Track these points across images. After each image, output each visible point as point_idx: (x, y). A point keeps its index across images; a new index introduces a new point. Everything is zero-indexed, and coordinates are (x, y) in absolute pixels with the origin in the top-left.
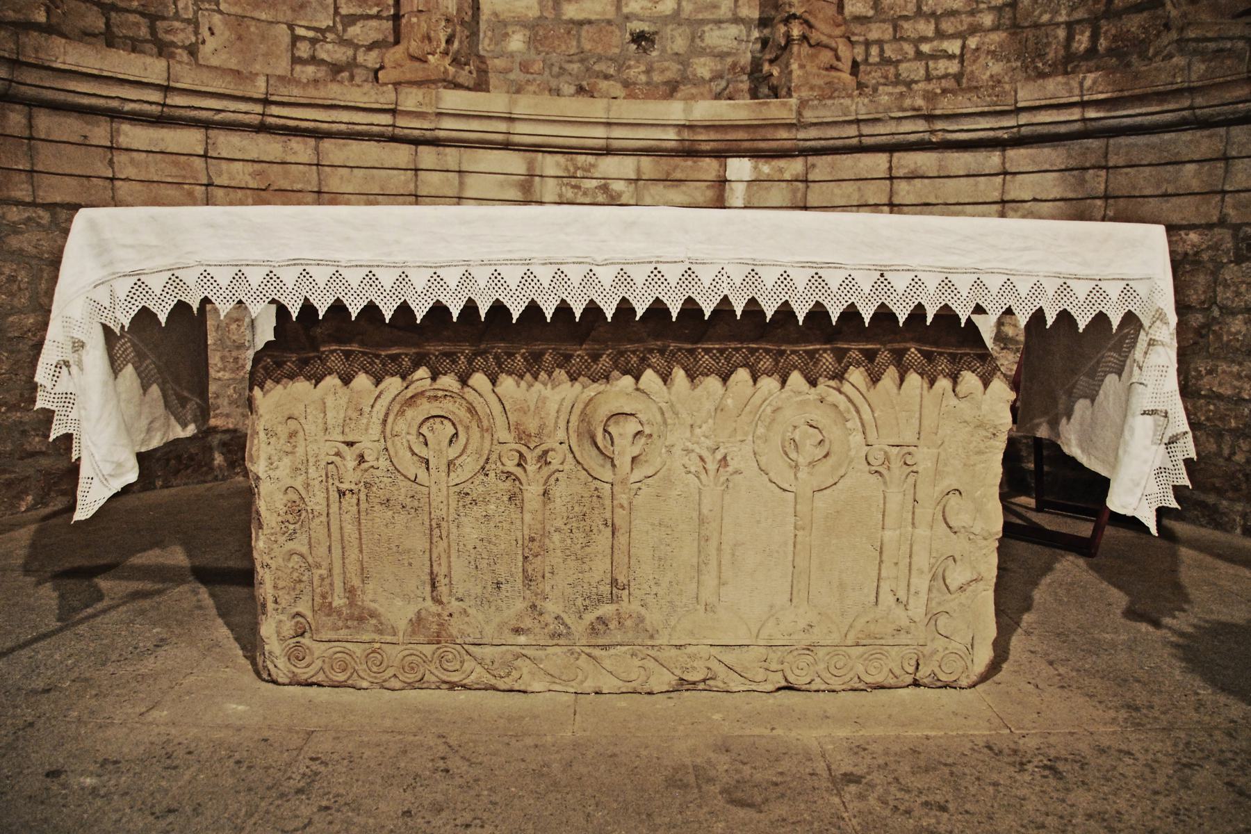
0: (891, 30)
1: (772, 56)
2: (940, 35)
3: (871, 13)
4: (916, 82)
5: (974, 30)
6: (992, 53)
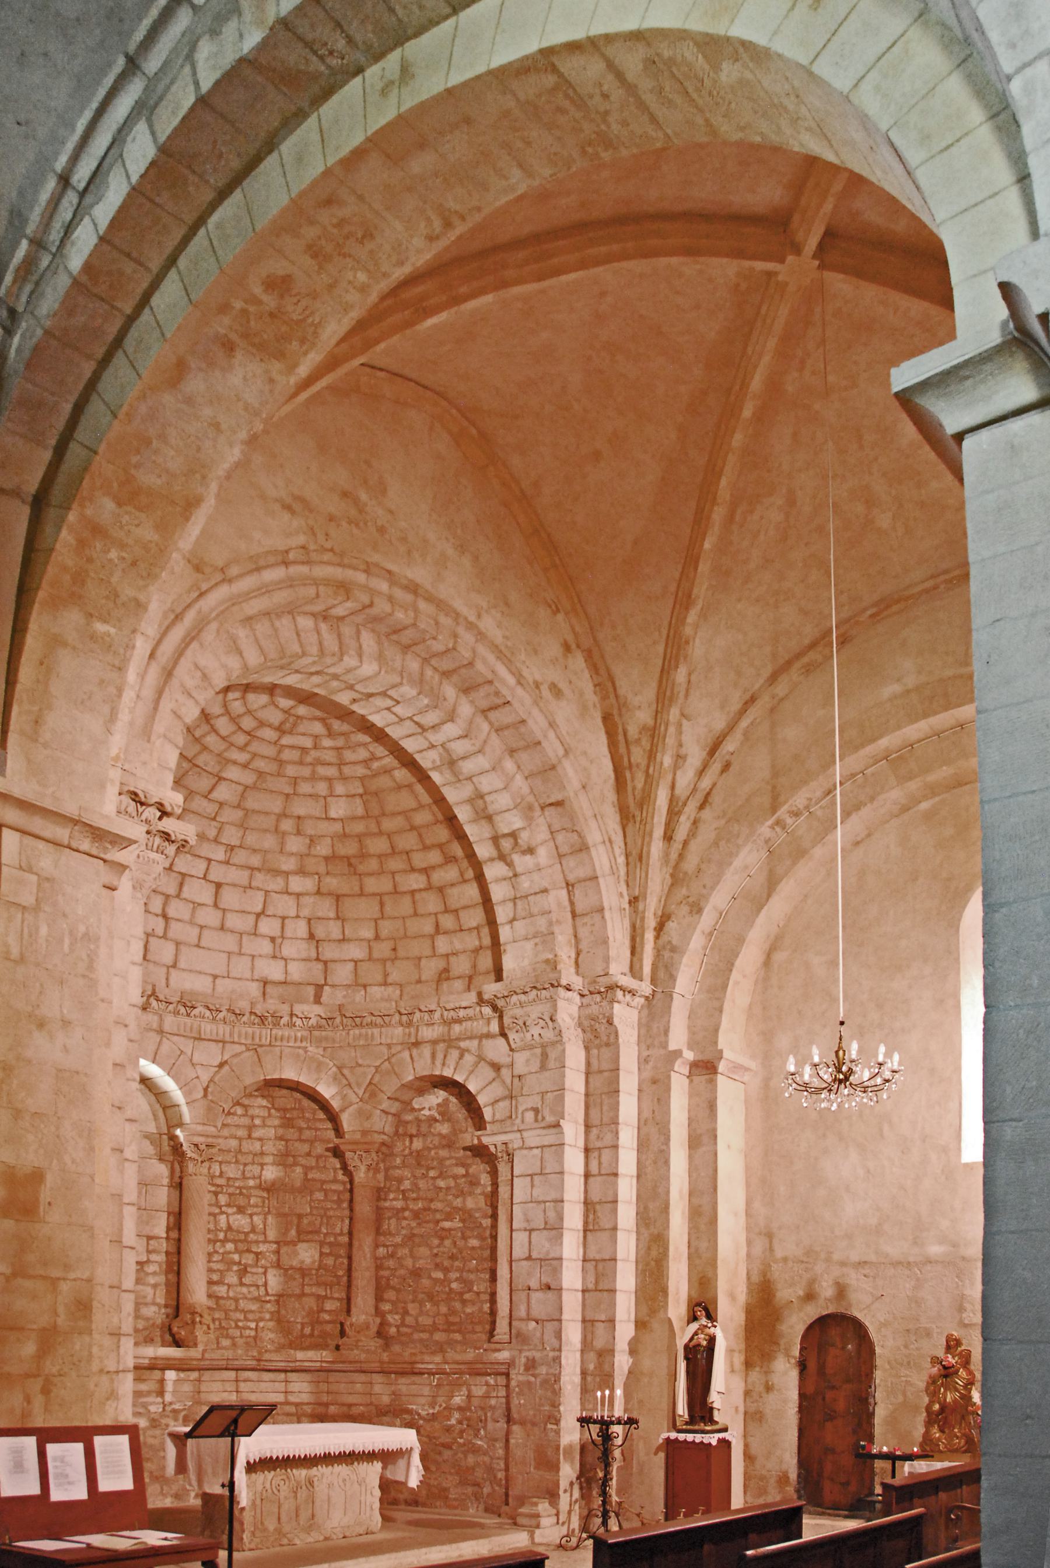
2: (246, 1319)
5: (262, 1319)
6: (270, 1330)
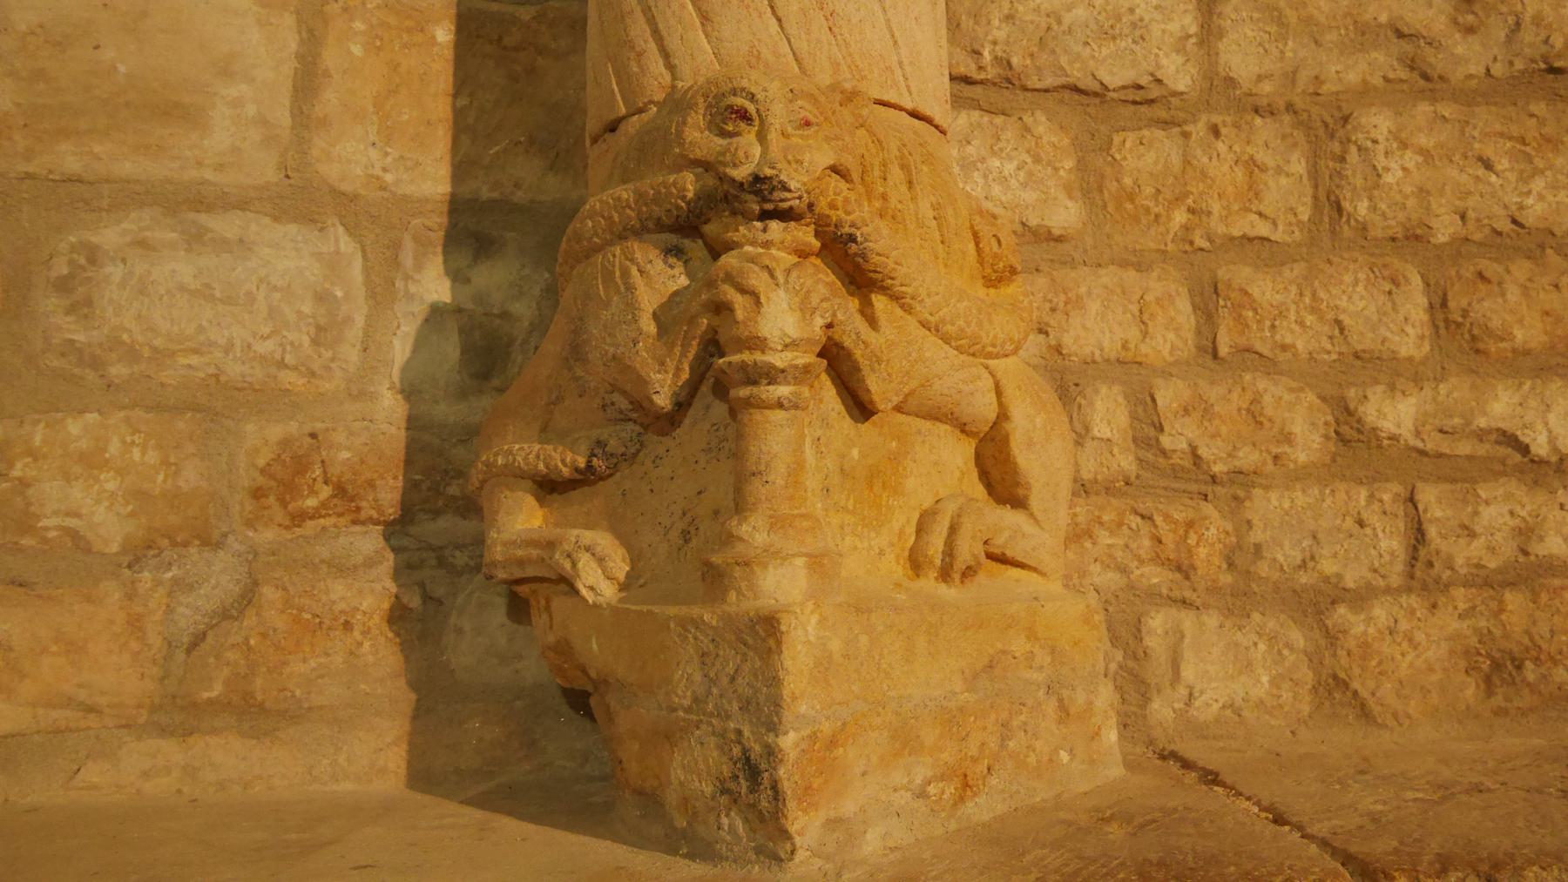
0: (1183, 308)
1: (565, 459)
3: (1066, 215)
4: (1360, 598)
